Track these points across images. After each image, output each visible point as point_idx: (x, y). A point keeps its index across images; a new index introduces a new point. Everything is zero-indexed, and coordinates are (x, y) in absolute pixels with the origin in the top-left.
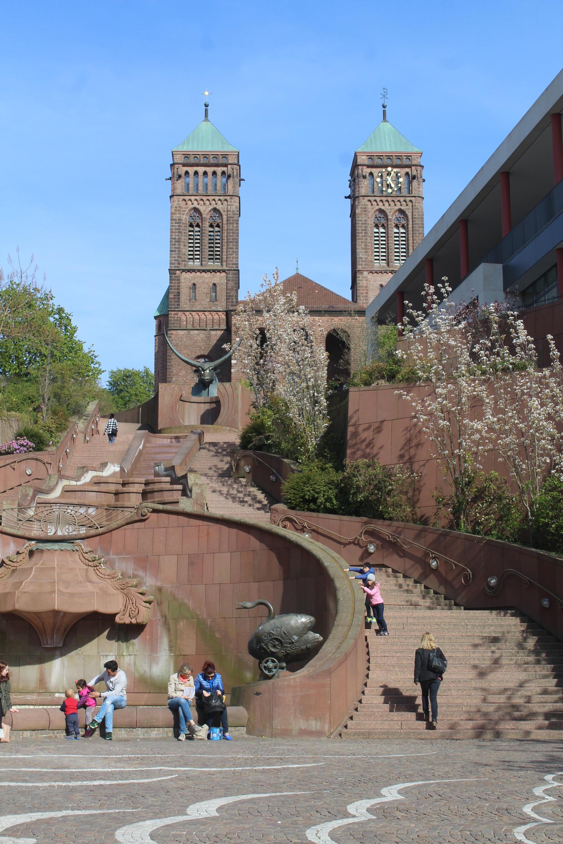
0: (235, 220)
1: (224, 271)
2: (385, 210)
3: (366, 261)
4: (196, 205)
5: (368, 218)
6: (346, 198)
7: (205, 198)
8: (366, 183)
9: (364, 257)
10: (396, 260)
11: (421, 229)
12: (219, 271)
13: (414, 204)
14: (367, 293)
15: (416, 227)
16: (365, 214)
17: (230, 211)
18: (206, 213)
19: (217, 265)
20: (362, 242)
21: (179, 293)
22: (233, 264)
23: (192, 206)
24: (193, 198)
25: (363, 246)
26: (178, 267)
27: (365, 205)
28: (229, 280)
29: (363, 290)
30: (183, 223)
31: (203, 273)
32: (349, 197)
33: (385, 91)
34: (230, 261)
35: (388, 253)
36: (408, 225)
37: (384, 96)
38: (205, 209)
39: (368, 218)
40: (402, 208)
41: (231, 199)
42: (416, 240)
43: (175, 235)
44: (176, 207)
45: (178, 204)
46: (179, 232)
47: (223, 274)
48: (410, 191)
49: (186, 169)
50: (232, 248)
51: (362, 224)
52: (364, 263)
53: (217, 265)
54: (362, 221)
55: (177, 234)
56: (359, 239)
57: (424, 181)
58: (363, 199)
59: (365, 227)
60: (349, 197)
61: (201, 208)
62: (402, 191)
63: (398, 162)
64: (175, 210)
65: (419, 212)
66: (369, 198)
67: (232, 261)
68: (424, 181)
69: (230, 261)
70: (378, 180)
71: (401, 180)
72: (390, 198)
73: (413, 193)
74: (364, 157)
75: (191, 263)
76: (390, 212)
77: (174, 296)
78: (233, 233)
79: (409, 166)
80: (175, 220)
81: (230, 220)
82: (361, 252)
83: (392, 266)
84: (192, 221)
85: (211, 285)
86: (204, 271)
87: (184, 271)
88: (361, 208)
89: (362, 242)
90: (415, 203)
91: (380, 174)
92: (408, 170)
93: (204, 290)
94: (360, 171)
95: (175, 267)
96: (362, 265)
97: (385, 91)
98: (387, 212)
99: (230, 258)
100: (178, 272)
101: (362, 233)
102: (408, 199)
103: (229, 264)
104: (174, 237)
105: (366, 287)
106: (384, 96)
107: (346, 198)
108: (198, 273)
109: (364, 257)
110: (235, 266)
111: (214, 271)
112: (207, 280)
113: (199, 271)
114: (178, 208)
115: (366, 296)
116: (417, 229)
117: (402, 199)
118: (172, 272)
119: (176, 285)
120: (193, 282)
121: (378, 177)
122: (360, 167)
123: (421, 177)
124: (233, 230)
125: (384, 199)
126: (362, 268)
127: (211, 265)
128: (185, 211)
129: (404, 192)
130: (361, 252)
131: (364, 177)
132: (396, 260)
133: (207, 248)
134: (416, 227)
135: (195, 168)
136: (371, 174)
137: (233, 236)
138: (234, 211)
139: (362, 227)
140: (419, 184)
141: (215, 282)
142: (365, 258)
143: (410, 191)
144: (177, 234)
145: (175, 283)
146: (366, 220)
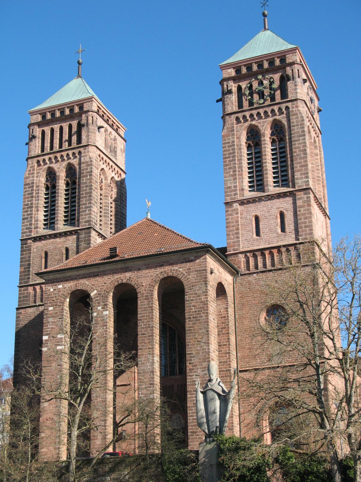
0: (88, 172)
2: (257, 124)
9: (233, 185)
11: (301, 138)
13: (291, 109)
17: (84, 163)
21: (29, 264)
22: (86, 222)
25: (232, 173)
26: (30, 235)
41: (85, 149)
51: (229, 146)
54: (229, 143)
58: (230, 117)
64: (29, 174)
65: (298, 118)
67: (85, 218)
72: (261, 110)
74: (229, 70)
76: (263, 126)
77: (25, 268)
80: (29, 184)
81: (83, 173)
89: (230, 168)
90: (293, 108)
93: (56, 258)
95: (27, 236)
100: (29, 241)
104: (27, 203)
110: (87, 224)
112: (60, 245)
116: (296, 138)
118: (24, 241)
119: (27, 256)
120: (44, 250)
122: (225, 83)
125: (254, 112)
126: (232, 199)
137: (86, 190)
138: (88, 162)
145: (26, 254)
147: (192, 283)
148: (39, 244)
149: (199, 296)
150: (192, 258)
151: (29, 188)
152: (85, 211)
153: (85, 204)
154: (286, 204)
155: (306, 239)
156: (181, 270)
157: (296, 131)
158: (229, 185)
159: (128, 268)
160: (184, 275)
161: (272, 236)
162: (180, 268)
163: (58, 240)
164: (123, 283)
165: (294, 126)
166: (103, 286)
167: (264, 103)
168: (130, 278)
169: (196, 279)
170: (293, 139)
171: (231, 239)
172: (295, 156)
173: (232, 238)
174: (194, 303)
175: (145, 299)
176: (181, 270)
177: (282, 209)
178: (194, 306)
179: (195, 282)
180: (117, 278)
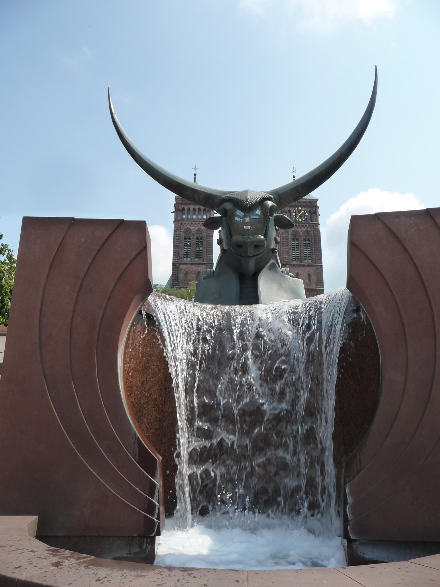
1: (204, 264)
4: (189, 226)
7: (194, 223)
12: (202, 264)
19: (200, 261)
21: (178, 276)
23: (186, 227)
24: (187, 222)
31: (192, 266)
38: (194, 229)
40: (308, 230)
47: (204, 266)
48: (311, 221)
49: (183, 206)
53: (200, 261)
61: (192, 228)
62: (308, 220)
63: (304, 204)
70: (294, 214)
71: (307, 214)
75: (185, 260)
79: (311, 206)
84: (186, 235)
85: (197, 272)
86: (193, 264)
87: (181, 264)
92: (310, 209)
100: (177, 264)
102: (311, 225)
108: (189, 266)
111: (199, 264)
113: (189, 264)
117: (308, 225)
125: (297, 224)
127: (197, 261)
129: (309, 221)
135: (189, 206)
136: (289, 211)
143: (311, 221)
148: (182, 267)
163: (193, 266)
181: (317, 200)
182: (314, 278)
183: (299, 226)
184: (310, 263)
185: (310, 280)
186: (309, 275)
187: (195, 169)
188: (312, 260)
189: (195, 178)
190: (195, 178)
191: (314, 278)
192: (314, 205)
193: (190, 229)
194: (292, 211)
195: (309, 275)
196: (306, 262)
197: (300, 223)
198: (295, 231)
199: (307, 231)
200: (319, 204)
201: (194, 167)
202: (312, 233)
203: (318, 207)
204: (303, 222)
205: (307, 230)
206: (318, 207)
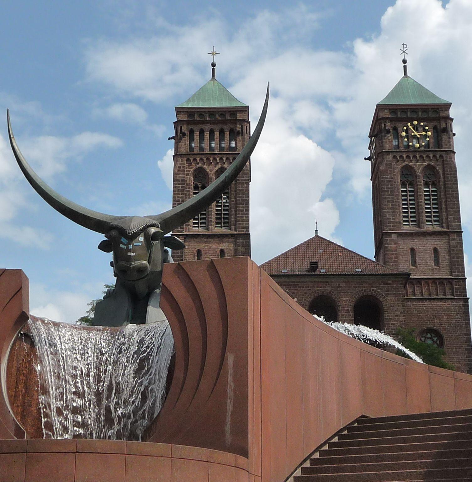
0: (245, 180)
2: (413, 166)
3: (393, 222)
5: (395, 175)
6: (366, 159)
8: (390, 138)
9: (391, 217)
10: (427, 221)
13: (445, 159)
14: (396, 258)
15: (448, 184)
16: (391, 171)
18: (212, 172)
20: (388, 201)
26: (181, 232)
27: (390, 161)
28: (239, 246)
29: (393, 254)
30: (187, 184)
32: (369, 159)
33: (405, 46)
34: (240, 224)
35: (419, 213)
36: (439, 182)
37: (404, 52)
39: (395, 175)
42: (449, 198)
43: (178, 197)
44: (179, 167)
45: (181, 164)
46: (183, 194)
50: (243, 211)
52: (392, 225)
54: (387, 178)
55: (180, 196)
56: (385, 198)
57: (454, 135)
59: (392, 185)
60: (369, 159)
64: (179, 171)
66: (394, 154)
67: (243, 224)
68: (454, 135)
69: (240, 224)
73: (444, 147)
78: (243, 194)
79: (439, 119)
80: (179, 181)
82: (388, 212)
83: (424, 227)
88: (386, 164)
90: (447, 158)
91: (405, 128)
94: (383, 125)
96: (390, 226)
97: (405, 46)
98: (415, 168)
99: (239, 221)
101: (388, 191)
103: (239, 228)
104: (177, 199)
105: (395, 251)
106: (404, 52)
107: (366, 159)
109: (391, 217)
110: (245, 230)
114: (182, 169)
115: (396, 261)
116: (450, 186)
120: (198, 248)
121: (404, 131)
123: (451, 131)
124: (242, 190)
128: (189, 171)
130: (388, 212)
131: (388, 132)
132: (427, 221)
133: (215, 211)
134: (448, 184)
135: (201, 126)
139: (387, 185)
140: (449, 138)
141: (223, 248)
142: (393, 219)
144: (180, 196)
146: (391, 178)
147: (391, 304)
149: (397, 316)
150: (390, 282)
151: (179, 185)
152: (243, 217)
153: (243, 211)
154: (440, 244)
155: (458, 275)
156: (380, 291)
157: (449, 179)
158: (388, 217)
159: (327, 282)
160: (383, 295)
161: (425, 269)
162: (379, 289)
164: (323, 295)
165: (448, 174)
166: (303, 295)
167: (419, 148)
168: (330, 291)
169: (393, 301)
170: (447, 186)
171: (390, 266)
172: (449, 201)
173: (391, 265)
174: (393, 321)
175: (346, 312)
176: (380, 291)
177: (435, 246)
178: (393, 324)
179: (393, 304)
180: (318, 290)
181: (451, 104)
182: (444, 256)
183: (415, 157)
184: (438, 228)
185: (437, 263)
186: (436, 250)
187: (213, 54)
188: (440, 222)
189: (213, 71)
190: (213, 71)
191: (444, 256)
192: (442, 114)
193: (204, 170)
194: (400, 130)
195: (436, 250)
196: (429, 228)
197: (416, 151)
198: (407, 168)
199: (429, 167)
200: (452, 113)
201: (211, 51)
202: (440, 171)
203: (452, 120)
204: (422, 149)
205: (429, 165)
206: (452, 120)
